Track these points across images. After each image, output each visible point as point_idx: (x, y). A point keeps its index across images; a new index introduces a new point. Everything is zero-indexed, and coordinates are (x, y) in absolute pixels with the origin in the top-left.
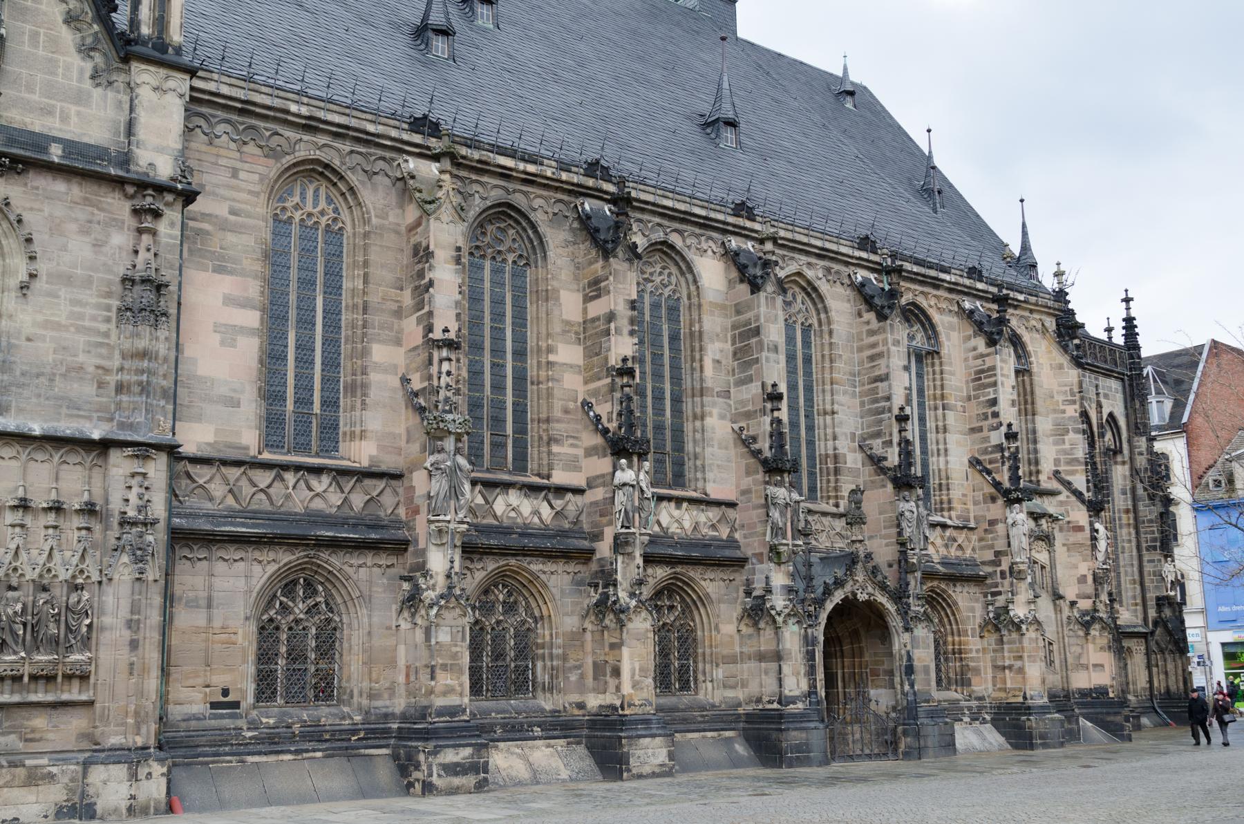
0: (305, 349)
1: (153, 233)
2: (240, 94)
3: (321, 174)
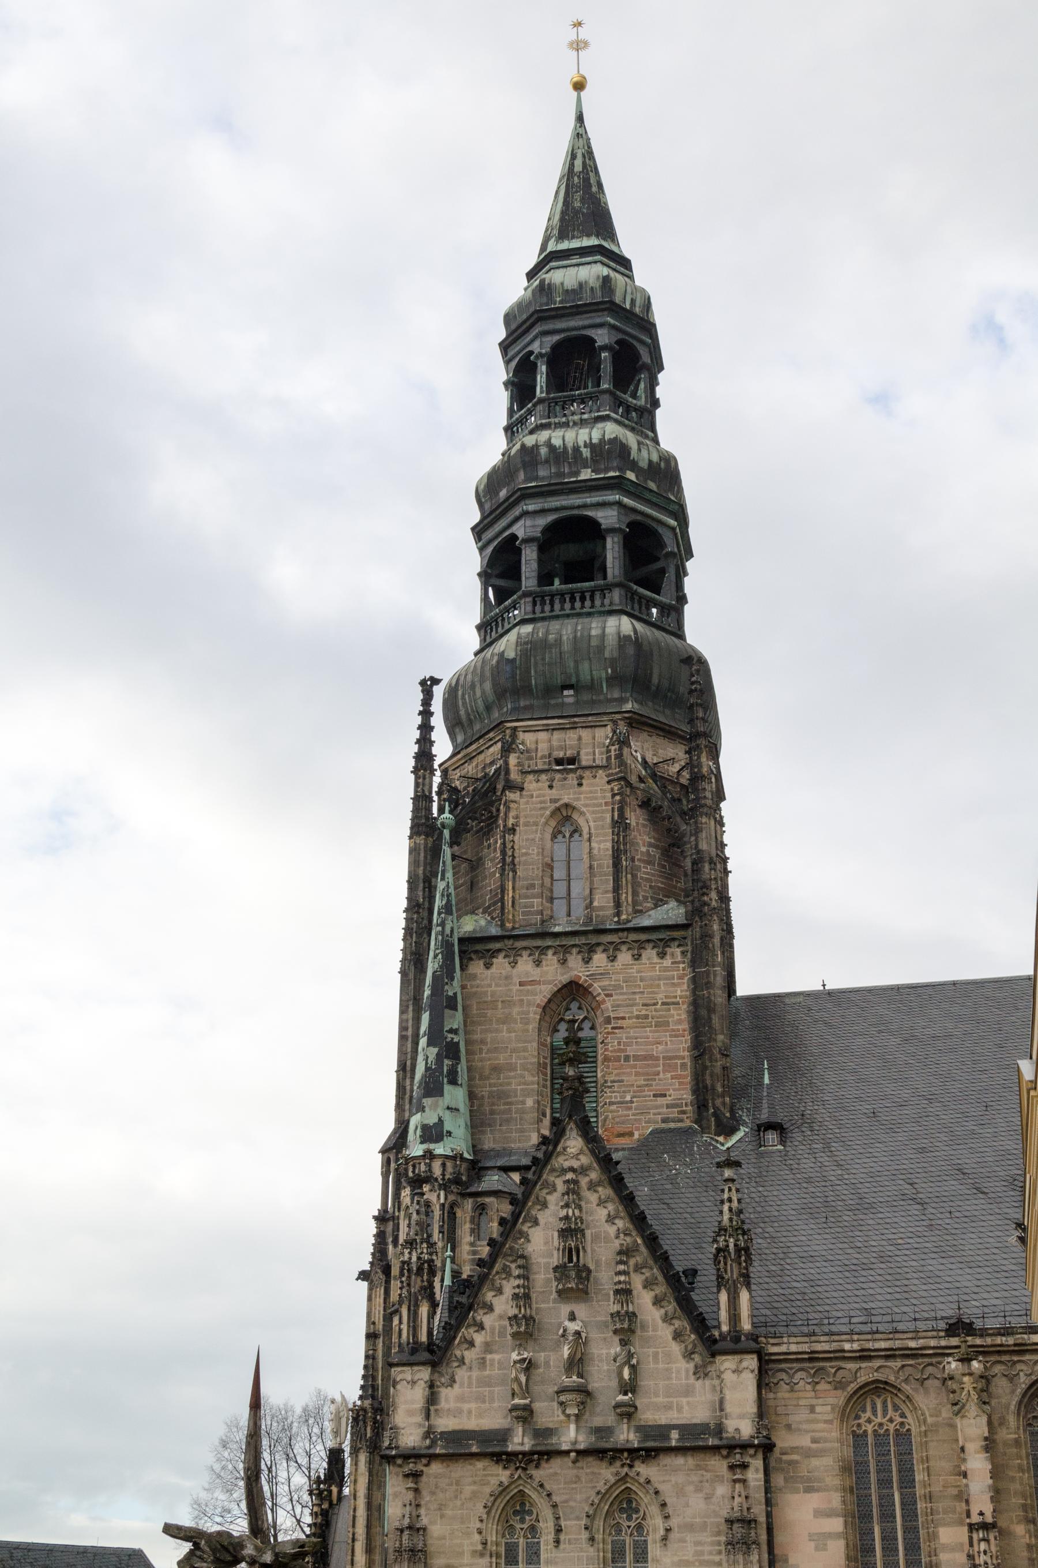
0: (889, 1539)
1: (744, 1481)
2: (805, 1348)
3: (884, 1389)
